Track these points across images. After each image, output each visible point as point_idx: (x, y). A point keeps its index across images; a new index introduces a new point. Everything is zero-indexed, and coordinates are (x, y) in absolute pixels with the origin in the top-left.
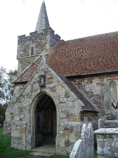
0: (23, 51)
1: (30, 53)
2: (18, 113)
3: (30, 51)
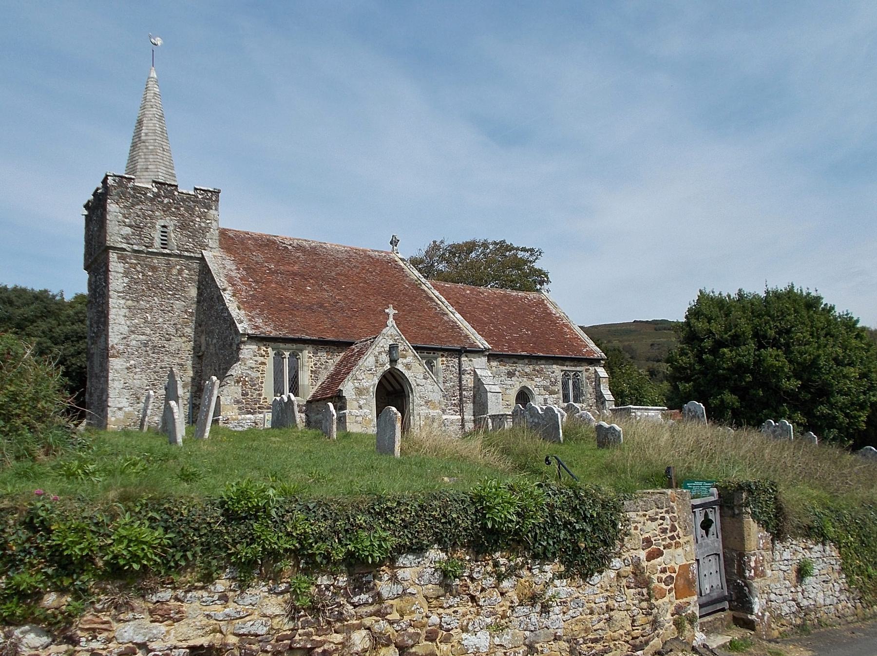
1: (157, 243)
2: (354, 397)
3: (157, 236)
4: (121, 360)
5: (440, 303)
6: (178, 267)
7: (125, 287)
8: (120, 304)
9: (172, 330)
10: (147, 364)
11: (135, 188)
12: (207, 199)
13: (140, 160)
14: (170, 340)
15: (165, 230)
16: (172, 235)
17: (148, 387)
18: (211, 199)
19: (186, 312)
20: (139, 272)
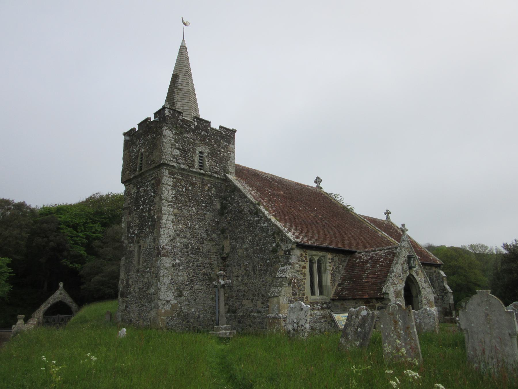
0: (179, 149)
1: (197, 165)
3: (196, 158)
4: (169, 259)
5: (368, 224)
6: (209, 185)
7: (173, 197)
8: (170, 211)
9: (204, 235)
10: (187, 262)
11: (183, 120)
12: (228, 136)
13: (178, 103)
14: (203, 243)
15: (202, 156)
16: (206, 160)
17: (188, 283)
18: (230, 136)
19: (214, 221)
20: (183, 187)
